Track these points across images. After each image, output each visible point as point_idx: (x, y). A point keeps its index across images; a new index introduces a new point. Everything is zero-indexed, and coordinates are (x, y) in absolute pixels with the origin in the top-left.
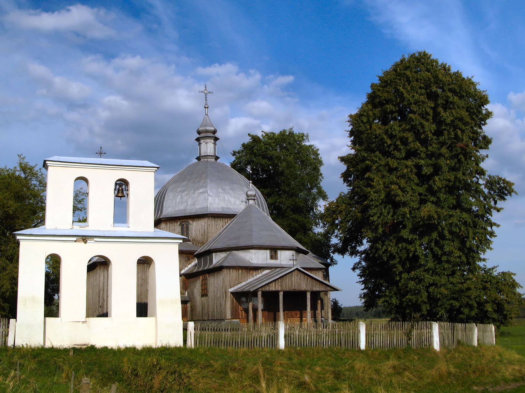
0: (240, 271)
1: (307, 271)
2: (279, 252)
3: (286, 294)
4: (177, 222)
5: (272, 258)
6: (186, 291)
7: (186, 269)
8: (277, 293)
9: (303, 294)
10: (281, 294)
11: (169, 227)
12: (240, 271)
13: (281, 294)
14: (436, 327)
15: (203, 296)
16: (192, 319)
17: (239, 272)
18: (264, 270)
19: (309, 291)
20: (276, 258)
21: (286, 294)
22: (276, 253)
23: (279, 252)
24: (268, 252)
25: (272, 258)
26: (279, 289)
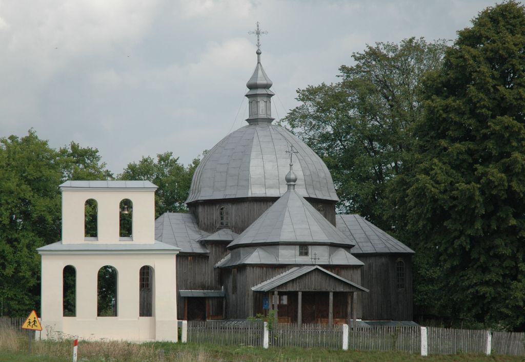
0: (265, 269)
1: (327, 270)
2: (310, 248)
3: (304, 293)
4: (216, 206)
5: (301, 254)
6: (221, 286)
7: (223, 260)
8: (296, 293)
9: (327, 294)
10: (300, 294)
12: (265, 269)
13: (300, 294)
14: (424, 330)
15: (233, 293)
16: (226, 317)
17: (263, 269)
18: (291, 268)
19: (331, 291)
20: (306, 254)
21: (304, 293)
22: (307, 249)
23: (310, 248)
24: (298, 247)
25: (301, 254)
26: (298, 290)
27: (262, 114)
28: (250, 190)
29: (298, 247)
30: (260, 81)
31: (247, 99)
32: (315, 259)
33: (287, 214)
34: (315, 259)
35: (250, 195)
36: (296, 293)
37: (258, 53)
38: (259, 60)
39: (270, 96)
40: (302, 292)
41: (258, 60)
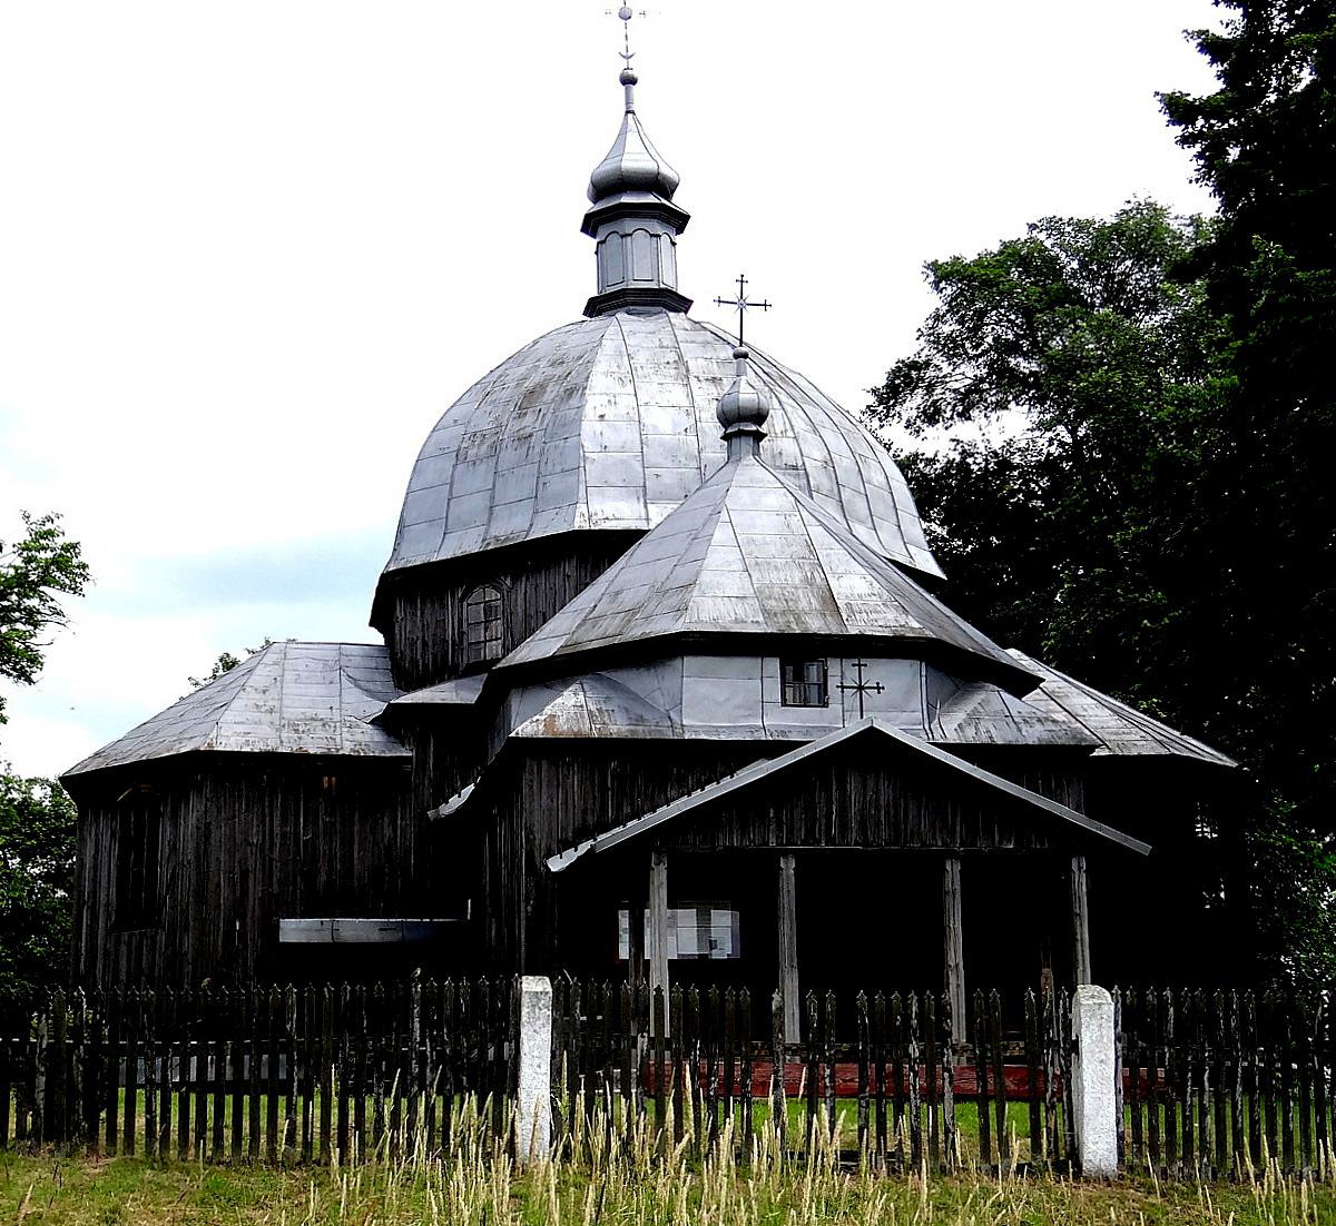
11: (422, 613)
13: (788, 867)
24: (773, 665)
26: (773, 843)
27: (640, 276)
28: (582, 508)
29: (773, 665)
30: (636, 161)
31: (590, 243)
32: (861, 688)
33: (721, 534)
34: (861, 688)
35: (580, 523)
36: (769, 862)
37: (628, 81)
38: (628, 102)
39: (679, 221)
40: (796, 853)
41: (627, 103)
